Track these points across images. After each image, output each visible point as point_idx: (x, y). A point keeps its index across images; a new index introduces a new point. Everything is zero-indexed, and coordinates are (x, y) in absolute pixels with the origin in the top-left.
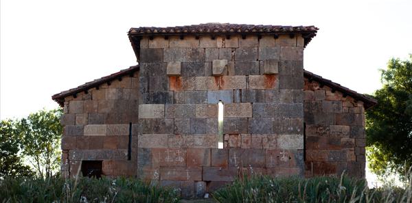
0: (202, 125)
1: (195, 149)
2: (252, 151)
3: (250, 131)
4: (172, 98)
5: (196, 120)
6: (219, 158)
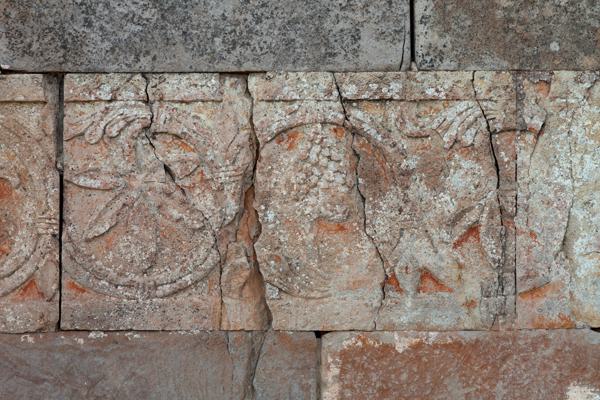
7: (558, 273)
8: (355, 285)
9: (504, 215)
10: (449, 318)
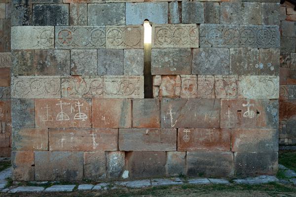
0: (116, 61)
1: (106, 99)
2: (198, 101)
3: (195, 71)
4: (67, 17)
5: (106, 52)
6: (145, 114)
7: (242, 94)
8: (223, 94)
9: (237, 88)
10: (232, 97)
